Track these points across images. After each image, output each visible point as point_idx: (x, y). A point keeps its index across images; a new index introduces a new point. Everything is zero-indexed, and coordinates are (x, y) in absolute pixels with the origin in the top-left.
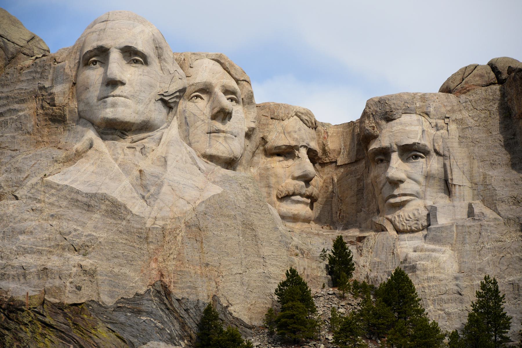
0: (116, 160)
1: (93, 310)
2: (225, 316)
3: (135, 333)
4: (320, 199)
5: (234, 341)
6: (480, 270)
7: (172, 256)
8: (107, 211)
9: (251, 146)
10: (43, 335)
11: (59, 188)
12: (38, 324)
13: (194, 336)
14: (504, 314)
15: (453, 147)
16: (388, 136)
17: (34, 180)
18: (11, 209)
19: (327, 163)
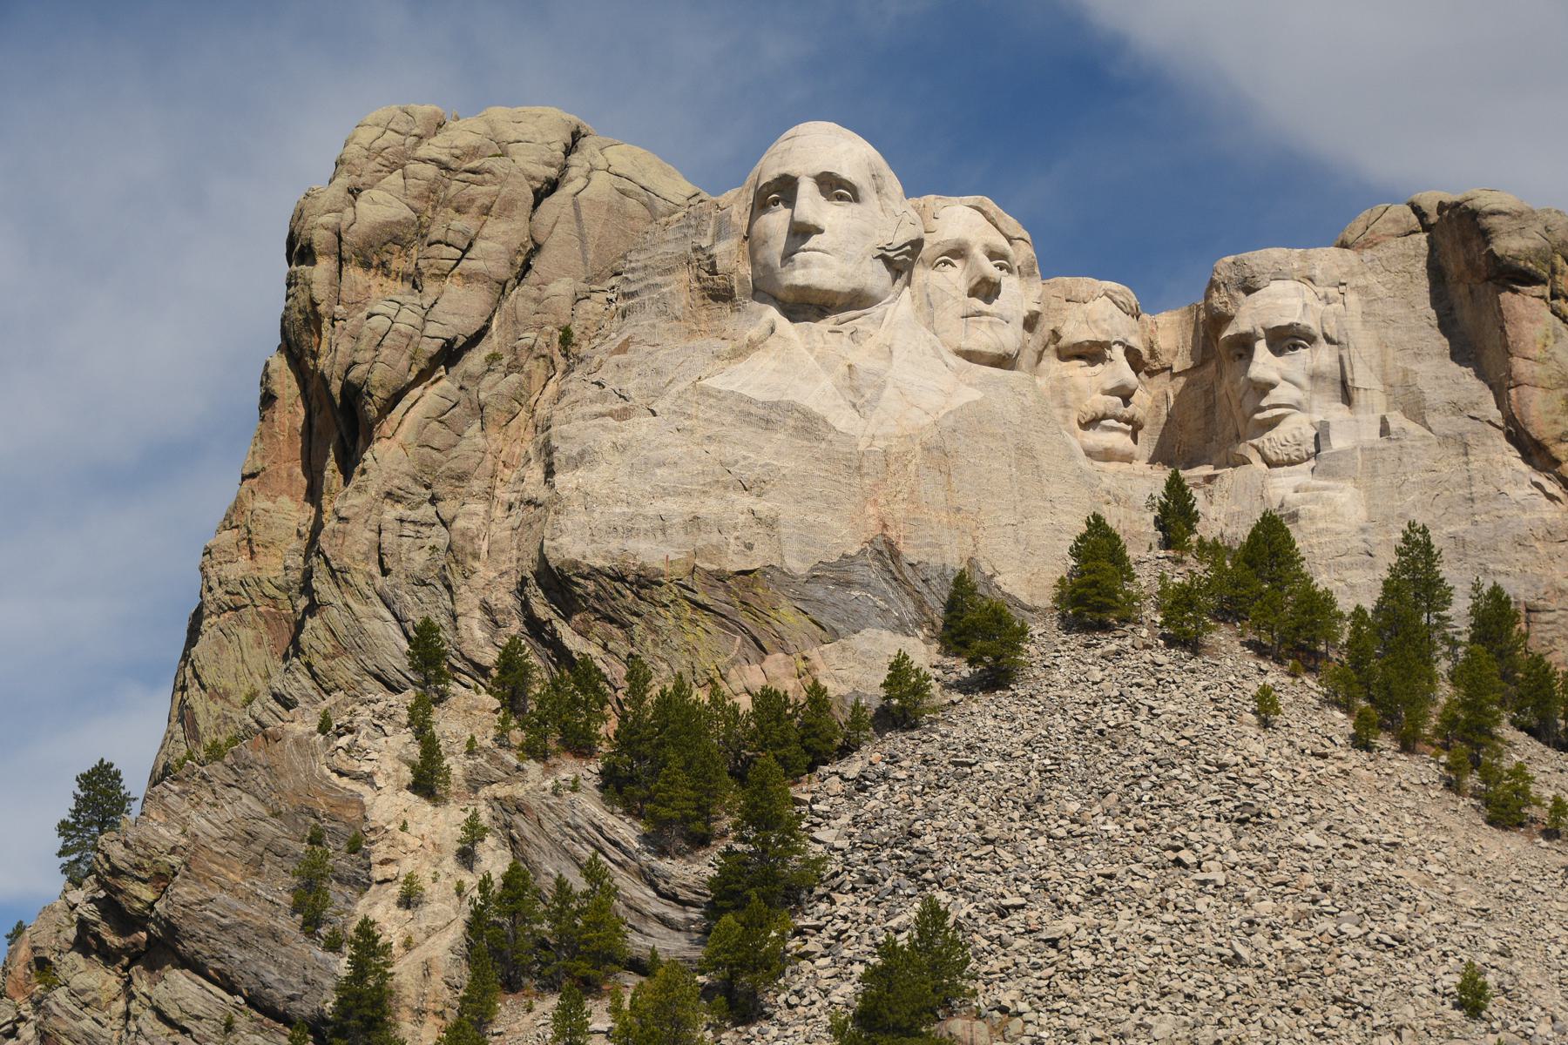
0: (811, 350)
1: (772, 580)
2: (990, 590)
3: (841, 615)
4: (1146, 427)
5: (999, 622)
6: (1401, 516)
7: (900, 496)
8: (795, 428)
9: (1035, 341)
10: (691, 621)
11: (720, 396)
12: (685, 604)
13: (939, 623)
14: (1442, 580)
16: (1249, 316)
17: (681, 386)
18: (644, 429)
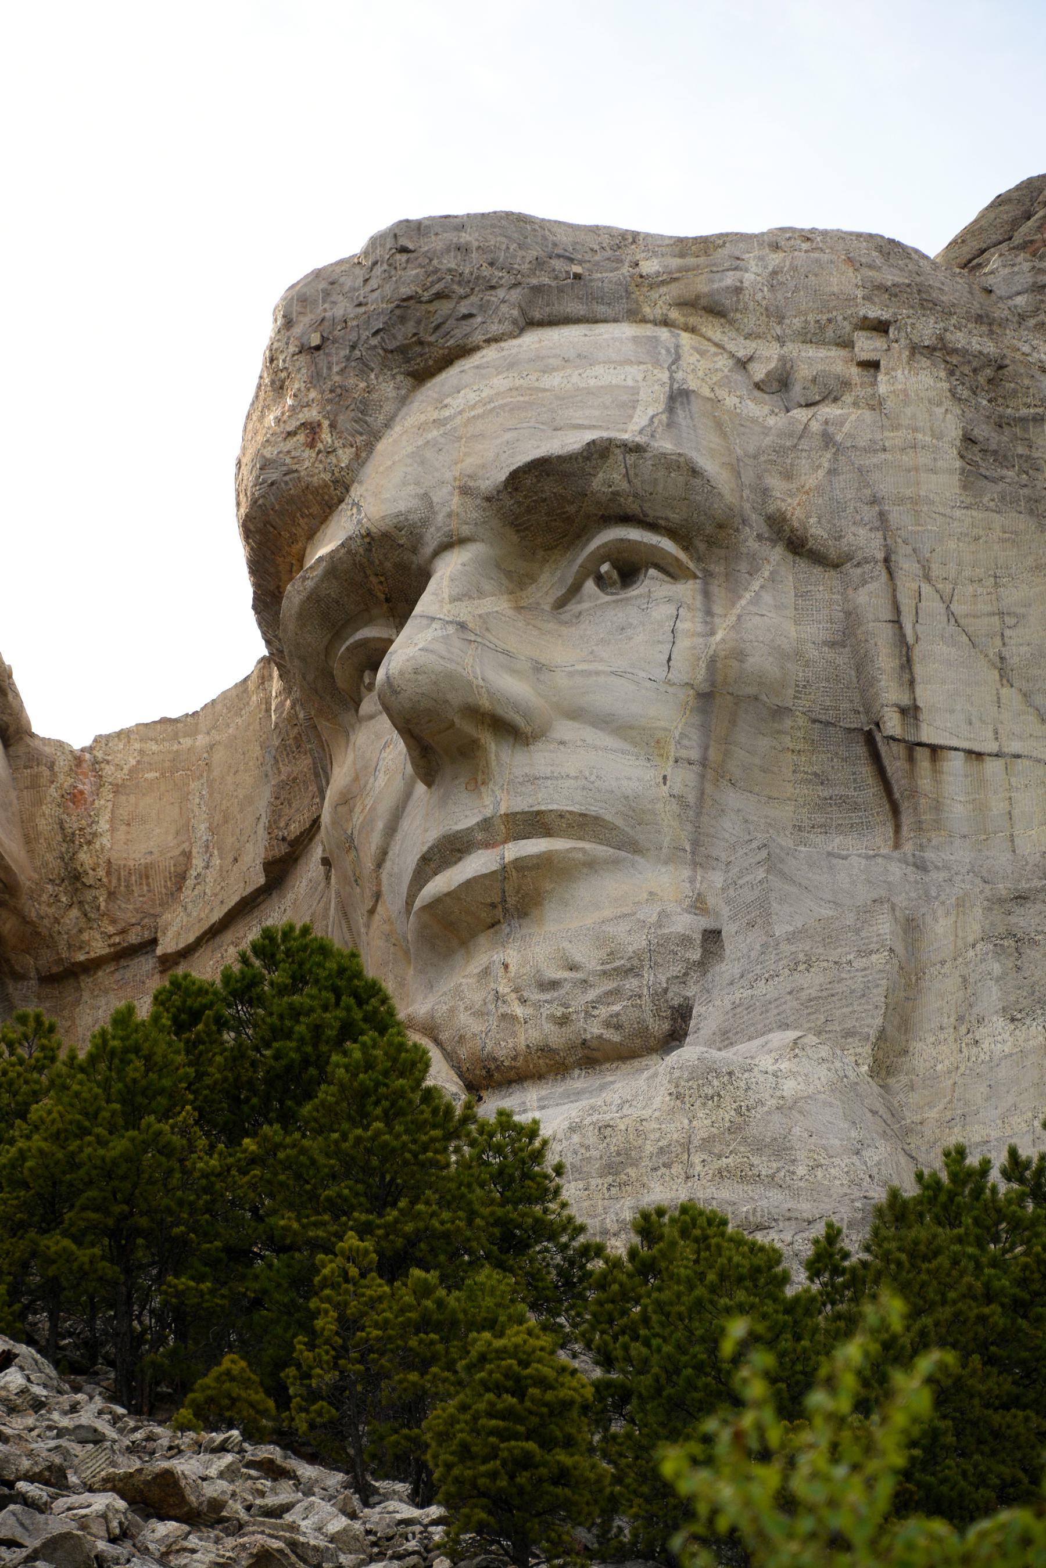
15: (915, 501)
19: (93, 965)
